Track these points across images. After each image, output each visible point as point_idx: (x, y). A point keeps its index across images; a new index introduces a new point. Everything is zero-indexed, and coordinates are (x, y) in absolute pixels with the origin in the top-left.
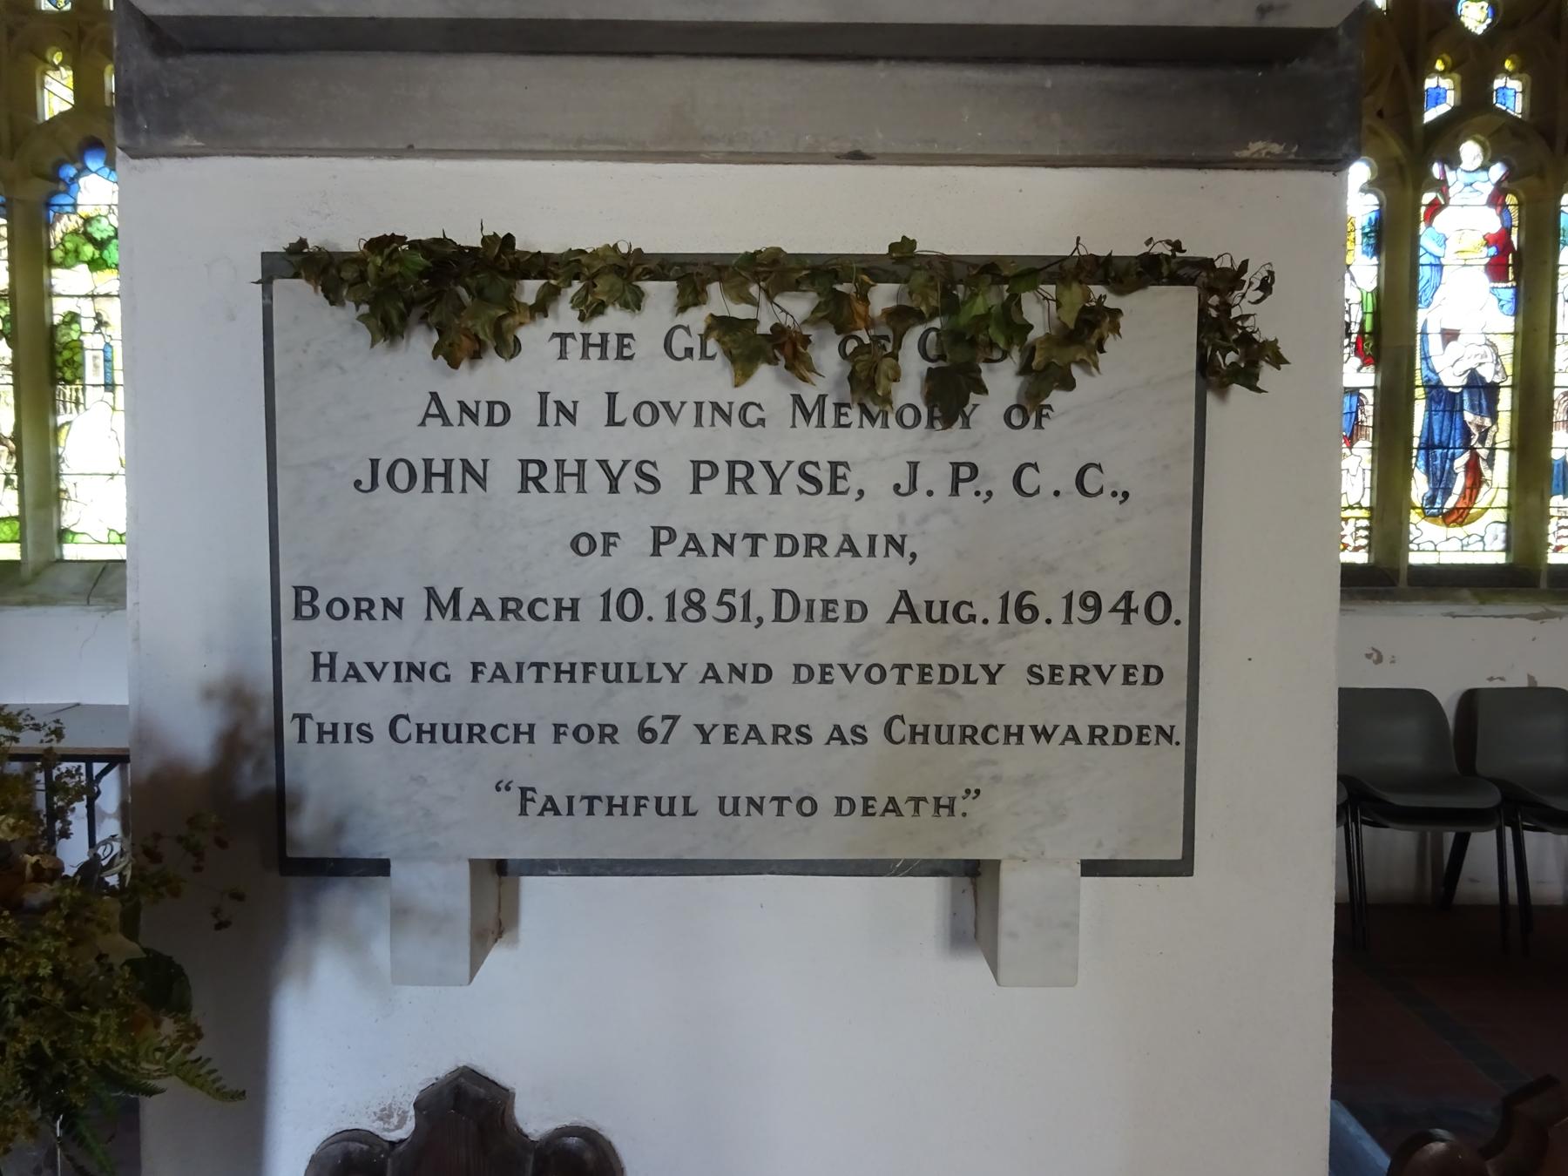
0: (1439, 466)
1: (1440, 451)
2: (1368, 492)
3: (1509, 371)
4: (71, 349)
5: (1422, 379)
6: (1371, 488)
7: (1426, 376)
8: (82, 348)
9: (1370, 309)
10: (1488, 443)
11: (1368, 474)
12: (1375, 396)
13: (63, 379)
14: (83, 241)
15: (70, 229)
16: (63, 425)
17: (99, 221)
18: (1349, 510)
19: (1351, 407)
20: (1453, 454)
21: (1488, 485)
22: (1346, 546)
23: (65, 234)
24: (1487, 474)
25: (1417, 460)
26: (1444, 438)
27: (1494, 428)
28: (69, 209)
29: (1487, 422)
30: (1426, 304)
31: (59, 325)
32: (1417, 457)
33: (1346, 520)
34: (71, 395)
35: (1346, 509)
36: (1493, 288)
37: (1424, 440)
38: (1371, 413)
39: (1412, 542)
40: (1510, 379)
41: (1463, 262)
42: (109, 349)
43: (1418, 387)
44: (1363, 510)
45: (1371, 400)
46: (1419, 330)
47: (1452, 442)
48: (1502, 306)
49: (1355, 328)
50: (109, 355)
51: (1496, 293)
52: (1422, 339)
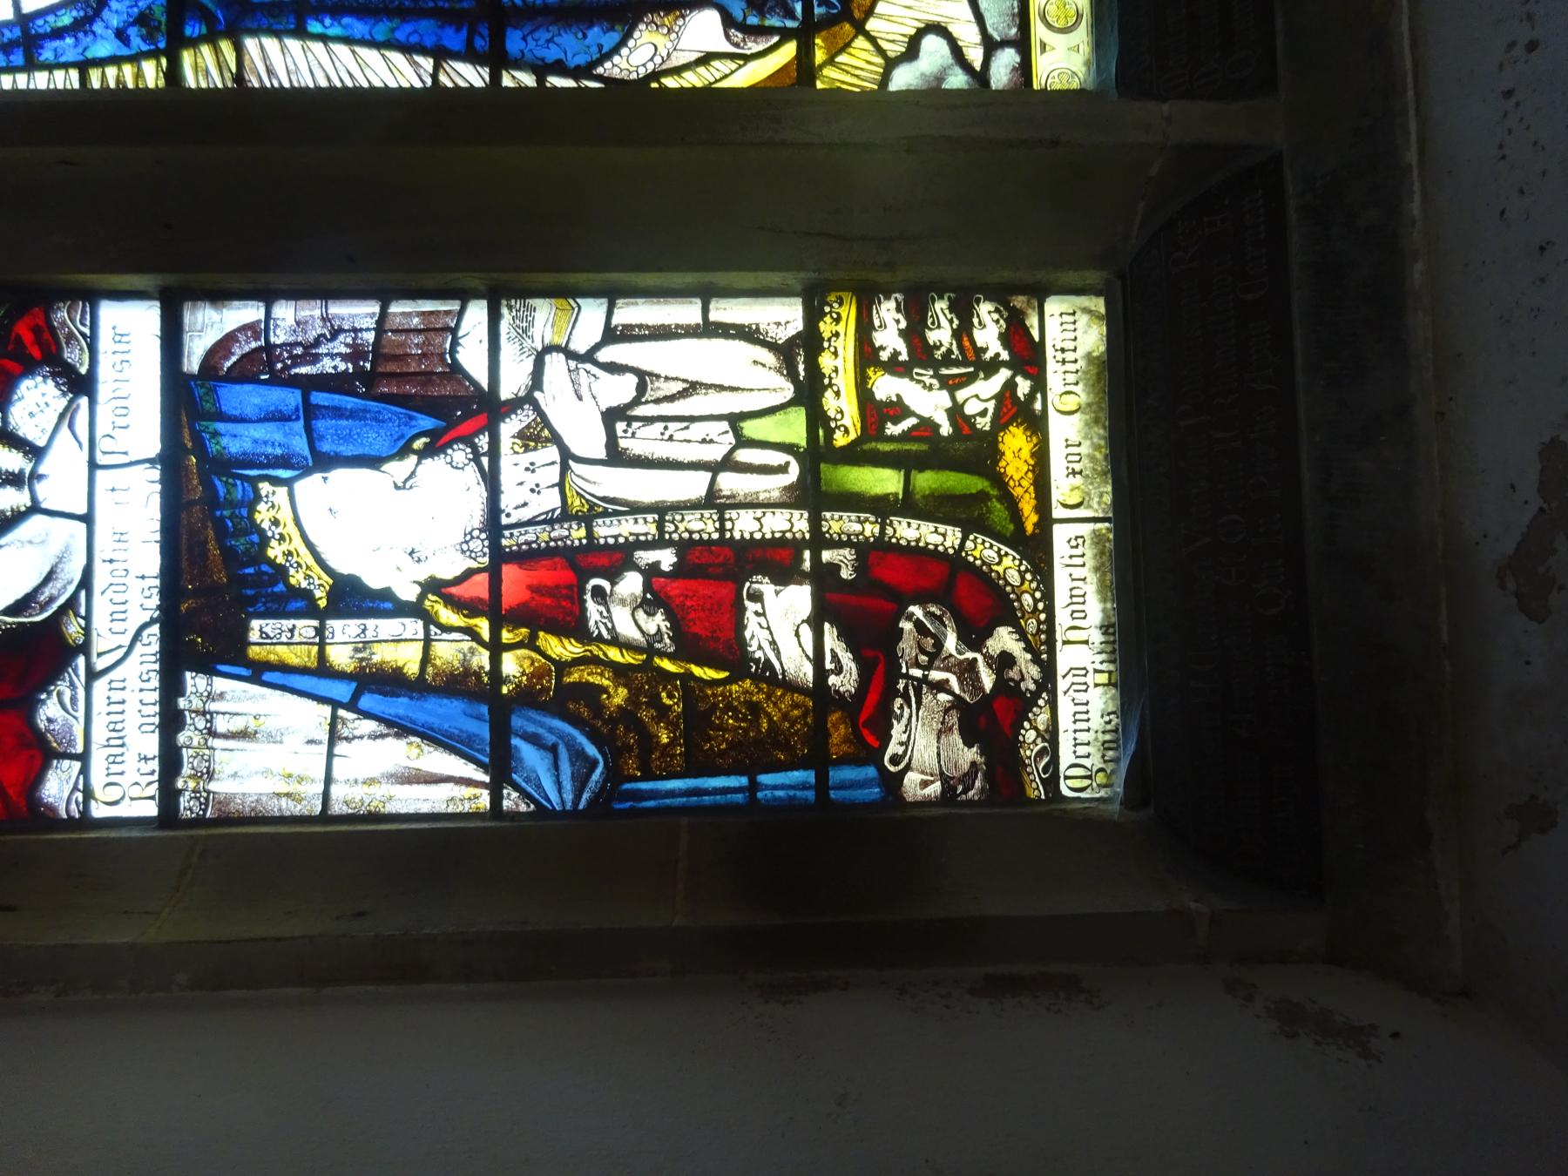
2: (727, 311)
5: (135, 59)
6: (706, 294)
7: (121, 35)
11: (631, 313)
12: (219, 296)
18: (830, 403)
19: (277, 417)
22: (1013, 410)
25: (560, 68)
32: (541, 70)
33: (875, 413)
35: (818, 420)
37: (454, 39)
38: (312, 310)
39: (981, 77)
43: (173, 74)
44: (826, 327)
45: (247, 313)
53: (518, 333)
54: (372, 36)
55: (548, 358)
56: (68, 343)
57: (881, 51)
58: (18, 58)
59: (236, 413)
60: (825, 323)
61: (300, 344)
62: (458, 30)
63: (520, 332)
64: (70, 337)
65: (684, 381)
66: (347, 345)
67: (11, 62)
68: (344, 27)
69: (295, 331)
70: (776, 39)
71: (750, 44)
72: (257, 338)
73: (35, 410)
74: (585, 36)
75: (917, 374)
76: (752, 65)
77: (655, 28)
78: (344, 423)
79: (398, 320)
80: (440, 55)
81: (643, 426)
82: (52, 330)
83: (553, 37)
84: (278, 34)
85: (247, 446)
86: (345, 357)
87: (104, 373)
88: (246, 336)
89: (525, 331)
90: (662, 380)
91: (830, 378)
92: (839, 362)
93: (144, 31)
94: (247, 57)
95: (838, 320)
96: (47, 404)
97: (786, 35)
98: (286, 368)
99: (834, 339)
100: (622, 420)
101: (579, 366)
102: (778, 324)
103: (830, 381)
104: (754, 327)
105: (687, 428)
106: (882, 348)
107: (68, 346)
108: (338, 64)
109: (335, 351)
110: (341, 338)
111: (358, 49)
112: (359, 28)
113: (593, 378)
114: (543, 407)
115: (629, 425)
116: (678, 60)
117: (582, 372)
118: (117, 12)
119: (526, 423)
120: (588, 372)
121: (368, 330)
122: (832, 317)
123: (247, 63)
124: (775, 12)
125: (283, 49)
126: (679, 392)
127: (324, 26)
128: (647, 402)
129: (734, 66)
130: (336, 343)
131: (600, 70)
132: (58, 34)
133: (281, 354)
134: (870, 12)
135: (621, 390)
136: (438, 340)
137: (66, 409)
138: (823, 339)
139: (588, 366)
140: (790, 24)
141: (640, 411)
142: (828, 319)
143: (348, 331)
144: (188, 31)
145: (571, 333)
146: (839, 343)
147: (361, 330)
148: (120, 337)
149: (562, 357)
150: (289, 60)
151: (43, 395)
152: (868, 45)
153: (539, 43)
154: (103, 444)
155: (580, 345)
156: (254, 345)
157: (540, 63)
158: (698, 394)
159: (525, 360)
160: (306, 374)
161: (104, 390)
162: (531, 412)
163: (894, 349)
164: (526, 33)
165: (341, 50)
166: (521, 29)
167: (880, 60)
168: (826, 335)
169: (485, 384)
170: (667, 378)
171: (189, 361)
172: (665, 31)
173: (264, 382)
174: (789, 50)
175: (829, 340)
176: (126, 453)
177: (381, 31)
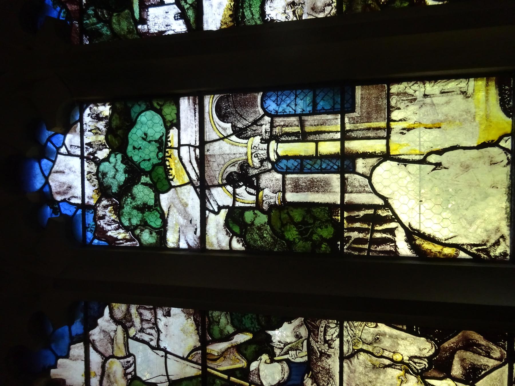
4: (283, 225)
8: (285, 205)
13: (332, 242)
14: (129, 200)
15: (114, 217)
16: (414, 247)
17: (104, 174)
23: (121, 226)
28: (90, 218)
31: (246, 243)
34: (360, 230)
42: (283, 164)
50: (291, 163)
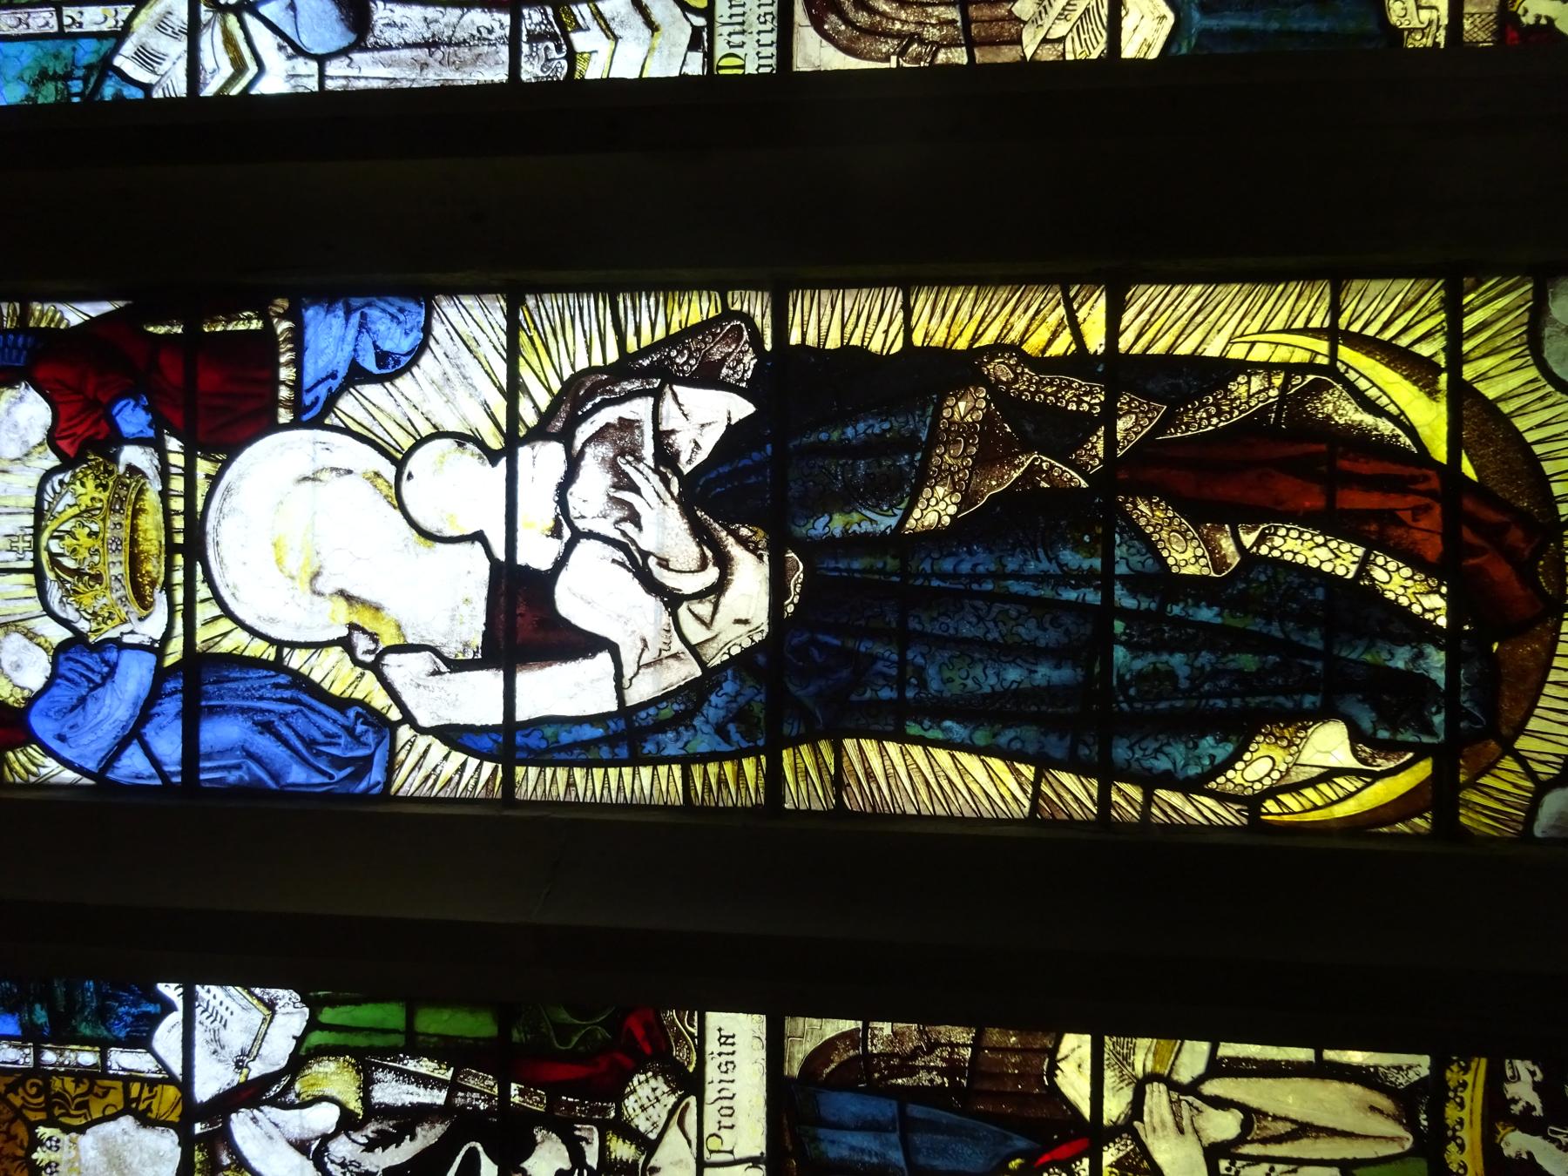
0: (1205, 658)
1: (1119, 653)
3: (697, 309)
5: (737, 756)
7: (721, 730)
9: (390, 1015)
10: (1085, 398)
20: (1135, 583)
21: (1317, 388)
24: (1249, 391)
25: (1171, 781)
26: (1049, 637)
27: (1000, 370)
29: (964, 408)
30: (370, 738)
36: (297, 406)
37: (1057, 747)
40: (740, 301)
41: (179, 560)
44: (1453, 1076)
45: (848, 1025)
46: (476, 776)
47: (1071, 595)
48: (382, 357)
49: (481, 1089)
51: (322, 391)
52: (541, 759)
53: (1119, 1060)
54: (971, 739)
55: (1148, 1088)
56: (676, 1042)
57: (1531, 774)
58: (623, 753)
59: (833, 1119)
60: (1452, 1071)
61: (896, 1055)
62: (1061, 738)
63: (1121, 1058)
64: (679, 1035)
65: (1293, 1121)
66: (943, 1059)
67: (616, 755)
68: (945, 730)
69: (892, 1042)
70: (1410, 755)
71: (1379, 761)
72: (855, 1048)
73: (646, 1103)
74: (1196, 746)
75: (1552, 1131)
76: (1379, 787)
77: (1274, 740)
78: (940, 1137)
79: (995, 1038)
80: (1044, 765)
81: (1248, 1165)
82: (663, 1028)
83: (1162, 746)
84: (880, 737)
85: (845, 1153)
86: (942, 1072)
87: (711, 1072)
88: (845, 1044)
89: (1126, 1058)
90: (1270, 1119)
91: (1455, 1130)
92: (1465, 1114)
93: (743, 728)
94: (845, 759)
95: (1466, 1070)
96: (657, 1098)
97: (1421, 753)
98: (883, 1078)
99: (1460, 1089)
100: (1226, 1158)
101: (1181, 1097)
102: (1399, 1068)
103: (1454, 1134)
104: (1372, 1070)
105: (1295, 1171)
106: (1515, 1101)
107: (676, 1046)
108: (937, 769)
109: (932, 1064)
110: (938, 1052)
111: (957, 754)
112: (958, 731)
113: (1195, 1111)
114: (1144, 1139)
115: (1232, 1164)
116: (1297, 776)
117: (1183, 1102)
118: (716, 707)
119: (1124, 1153)
120: (1190, 1105)
121: (965, 1045)
122: (1460, 1066)
123: (845, 764)
124: (1410, 726)
125: (883, 752)
126: (1287, 1133)
127: (923, 728)
128: (1252, 1142)
129: (1359, 784)
130: (933, 1056)
131: (1213, 785)
132: (661, 726)
133: (879, 1063)
134: (1520, 730)
135: (1224, 1126)
136: (1036, 1062)
137: (676, 1106)
138: (1448, 1089)
139: (1190, 1099)
140: (1426, 739)
141: (1247, 1150)
142: (1455, 1068)
143: (945, 1045)
144: (786, 730)
145: (1173, 1064)
146: (1466, 1095)
147: (958, 1045)
148: (725, 1039)
149: (1163, 1087)
150: (887, 763)
151: (654, 1090)
152: (1515, 767)
153: (1147, 753)
154: (713, 1144)
155: (1184, 1076)
156: (852, 1053)
157: (1147, 774)
158: (1308, 1137)
159: (1126, 1088)
160: (903, 1085)
161: (711, 1093)
162: (1129, 1142)
163: (1527, 1103)
164: (1133, 741)
165: (942, 756)
166: (1127, 738)
167: (1529, 784)
168: (1452, 1084)
169: (1086, 1110)
170: (1276, 1118)
171: (790, 1066)
172: (1285, 743)
173: (861, 1091)
174: (1423, 769)
175: (1455, 1090)
176: (731, 1152)
177: (981, 738)
